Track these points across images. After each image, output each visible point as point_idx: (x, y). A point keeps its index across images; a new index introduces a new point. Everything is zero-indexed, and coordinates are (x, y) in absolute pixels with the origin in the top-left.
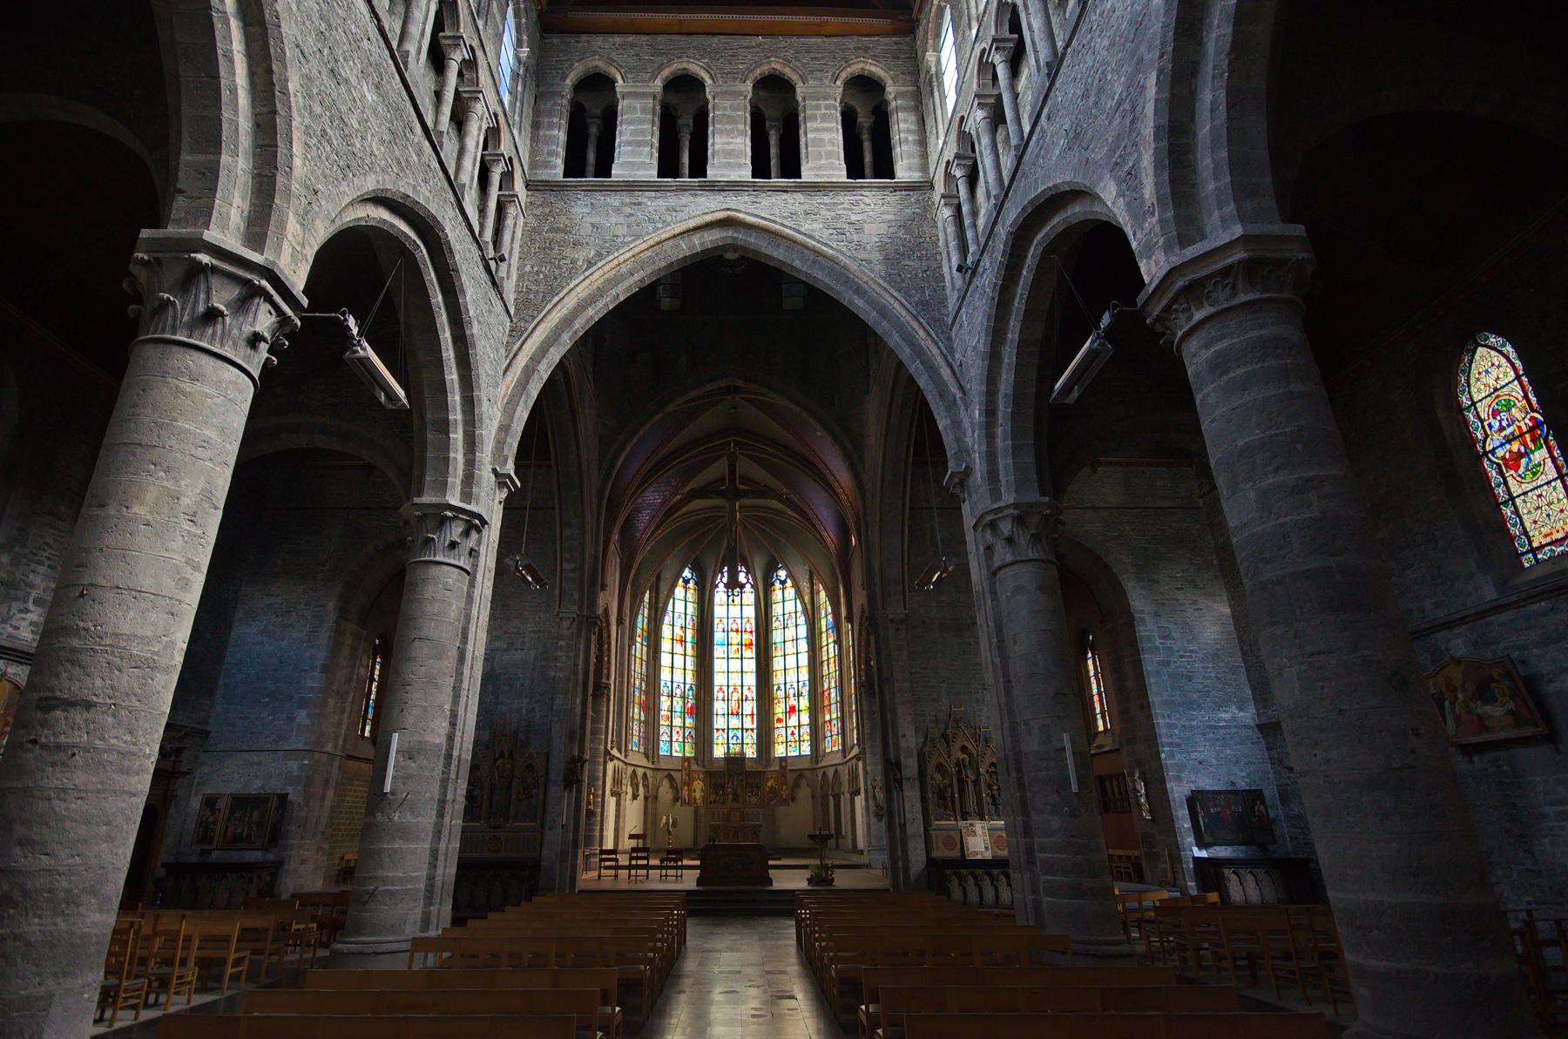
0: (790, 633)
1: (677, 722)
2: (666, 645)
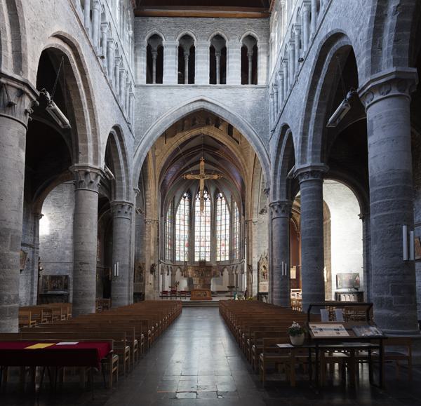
0: (223, 217)
1: (182, 249)
2: (177, 222)
